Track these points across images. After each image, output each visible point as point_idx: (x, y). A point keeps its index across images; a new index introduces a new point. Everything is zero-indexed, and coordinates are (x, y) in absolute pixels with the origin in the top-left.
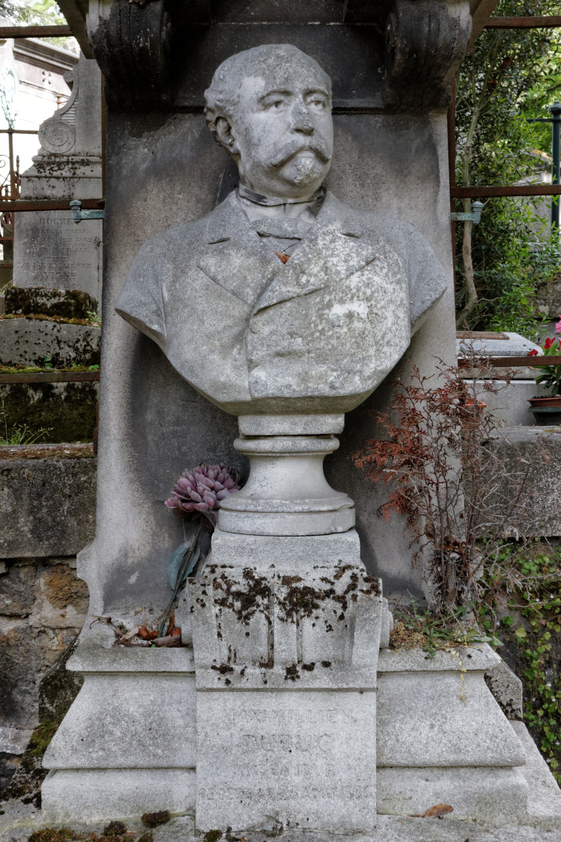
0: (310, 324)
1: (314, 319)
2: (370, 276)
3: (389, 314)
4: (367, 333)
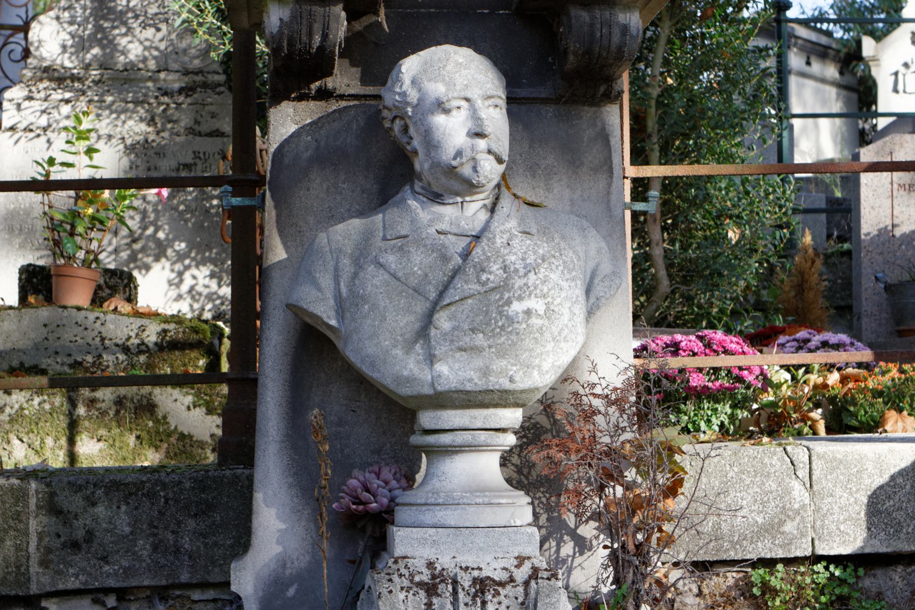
0: (491, 320)
1: (494, 315)
2: (547, 273)
3: (566, 311)
4: (544, 329)
